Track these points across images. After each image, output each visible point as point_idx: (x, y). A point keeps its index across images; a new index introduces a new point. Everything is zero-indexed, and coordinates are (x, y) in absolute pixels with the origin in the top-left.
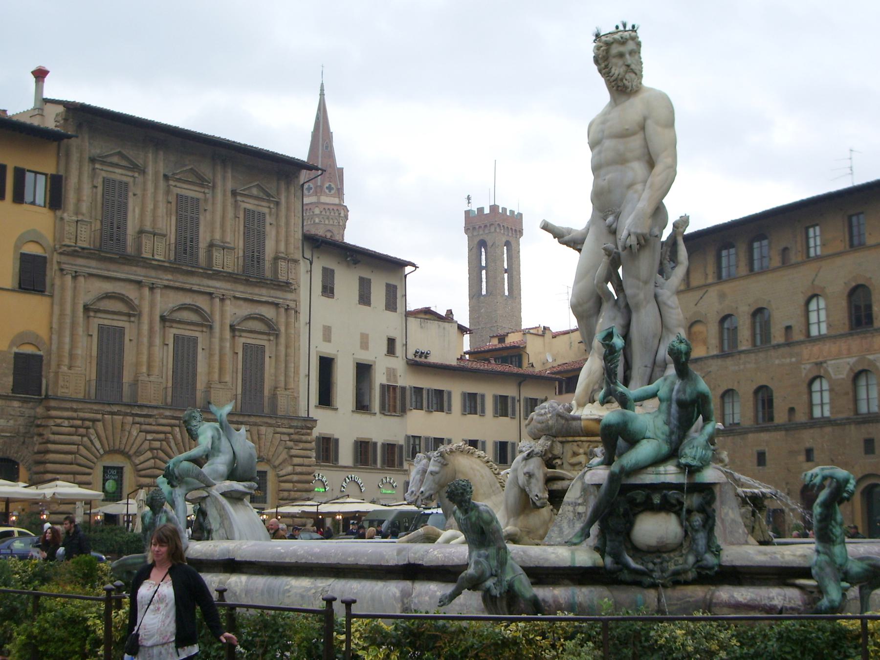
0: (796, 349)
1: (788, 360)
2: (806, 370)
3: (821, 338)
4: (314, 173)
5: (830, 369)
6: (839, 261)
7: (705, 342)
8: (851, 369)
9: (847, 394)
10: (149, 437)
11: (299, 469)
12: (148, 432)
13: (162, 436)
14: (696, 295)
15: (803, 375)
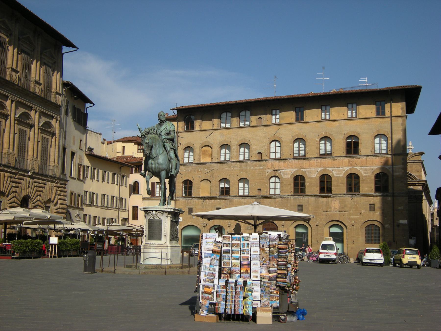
0: (264, 163)
1: (258, 168)
2: (269, 172)
3: (276, 159)
4: (71, 49)
5: (281, 173)
6: (289, 127)
7: (211, 156)
8: (293, 174)
9: (290, 185)
10: (14, 185)
11: (61, 206)
12: (13, 182)
13: (17, 185)
14: (208, 133)
15: (267, 175)
